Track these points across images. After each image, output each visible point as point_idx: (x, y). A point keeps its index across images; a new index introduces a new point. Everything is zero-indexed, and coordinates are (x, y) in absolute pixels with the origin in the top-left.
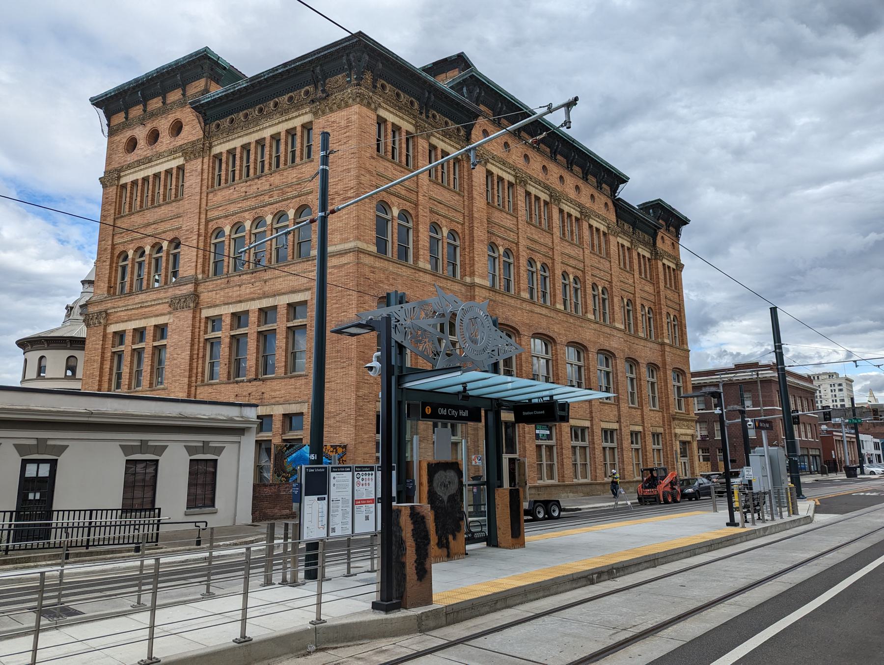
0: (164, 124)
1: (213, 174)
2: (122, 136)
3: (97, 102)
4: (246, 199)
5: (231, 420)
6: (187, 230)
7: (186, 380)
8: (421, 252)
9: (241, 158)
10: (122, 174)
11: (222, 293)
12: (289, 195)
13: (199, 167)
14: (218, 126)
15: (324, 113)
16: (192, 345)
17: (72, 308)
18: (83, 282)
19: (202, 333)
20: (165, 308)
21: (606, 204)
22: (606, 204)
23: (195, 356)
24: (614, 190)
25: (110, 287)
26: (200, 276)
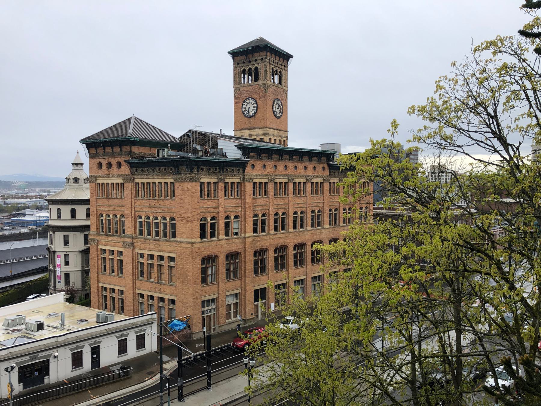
0: (114, 162)
4: (149, 207)
8: (220, 232)
9: (147, 188)
11: (143, 245)
12: (167, 211)
13: (130, 187)
14: (136, 170)
15: (178, 182)
16: (133, 263)
17: (69, 179)
18: (73, 164)
20: (121, 245)
21: (323, 167)
22: (323, 167)
26: (134, 235)
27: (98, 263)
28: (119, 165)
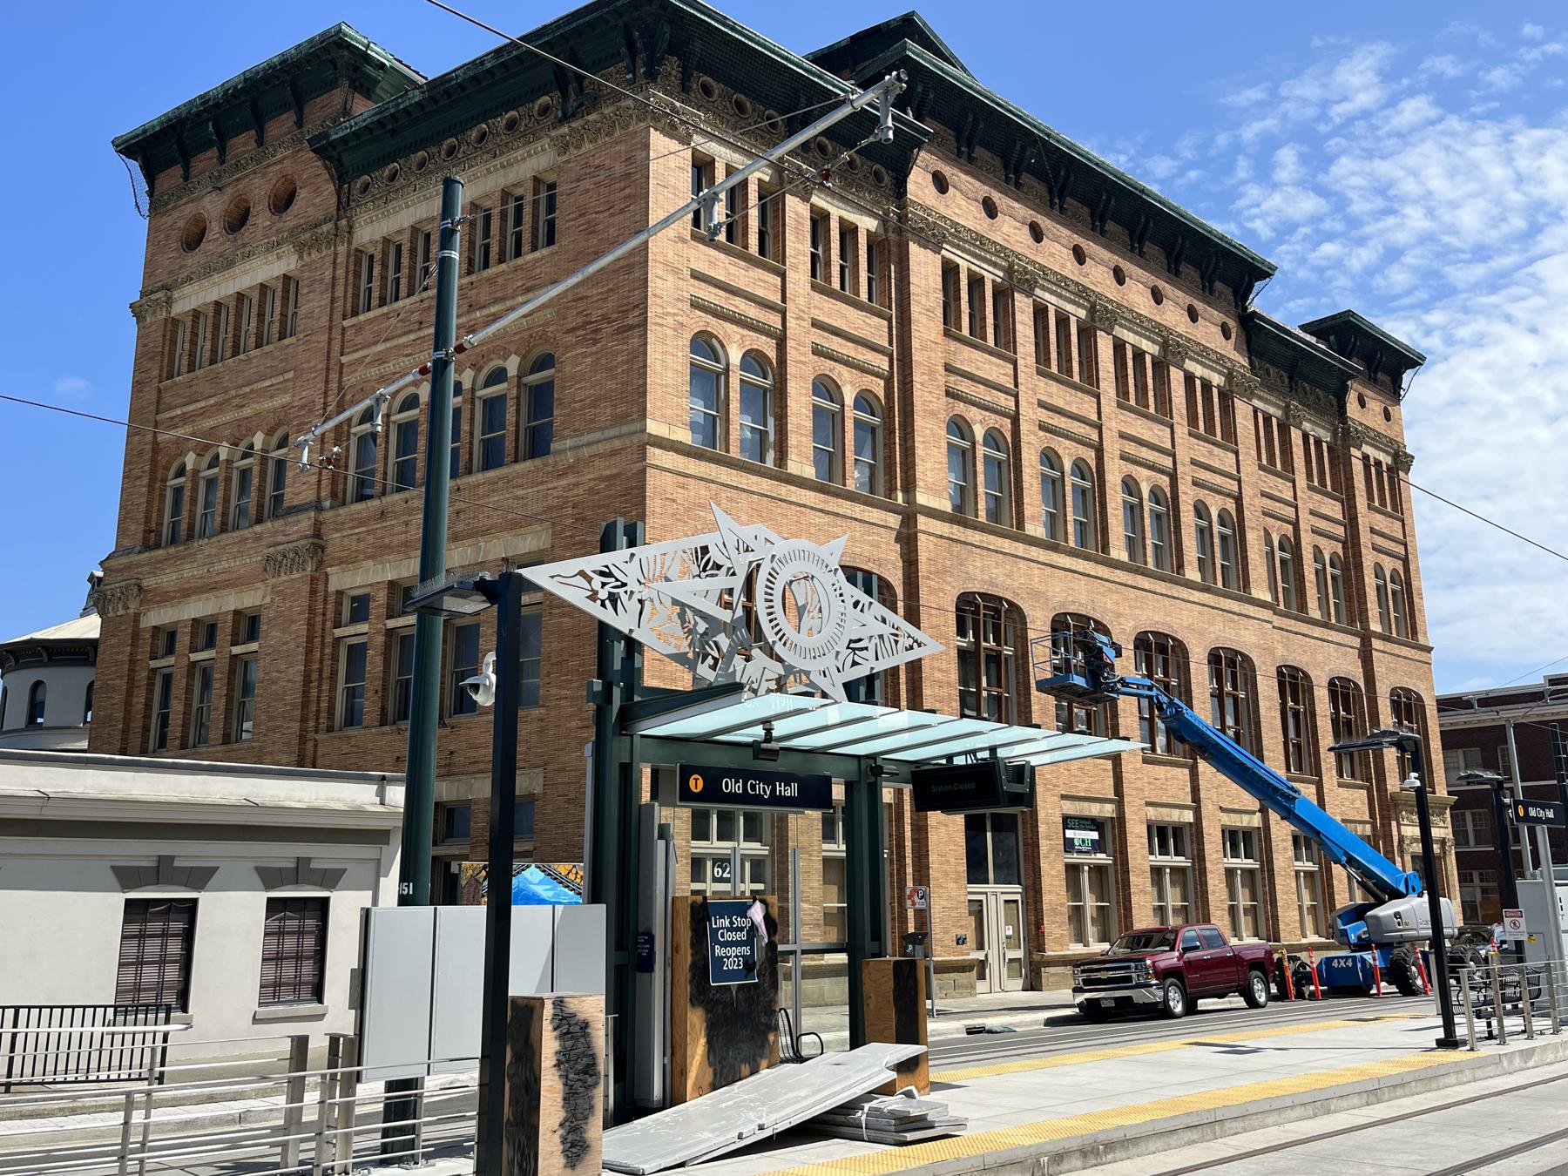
1: (357, 287)
2: (176, 214)
3: (131, 147)
5: (359, 812)
6: (302, 407)
7: (296, 726)
8: (792, 440)
10: (176, 294)
11: (370, 539)
13: (328, 274)
16: (309, 652)
19: (329, 624)
23: (315, 676)
24: (1242, 293)
25: (148, 531)
27: (128, 703)
28: (283, 202)
